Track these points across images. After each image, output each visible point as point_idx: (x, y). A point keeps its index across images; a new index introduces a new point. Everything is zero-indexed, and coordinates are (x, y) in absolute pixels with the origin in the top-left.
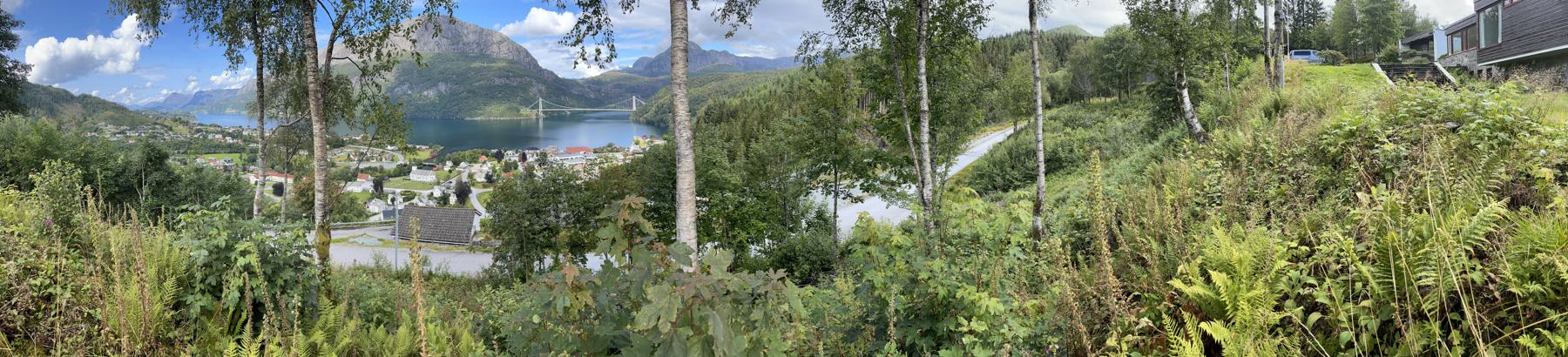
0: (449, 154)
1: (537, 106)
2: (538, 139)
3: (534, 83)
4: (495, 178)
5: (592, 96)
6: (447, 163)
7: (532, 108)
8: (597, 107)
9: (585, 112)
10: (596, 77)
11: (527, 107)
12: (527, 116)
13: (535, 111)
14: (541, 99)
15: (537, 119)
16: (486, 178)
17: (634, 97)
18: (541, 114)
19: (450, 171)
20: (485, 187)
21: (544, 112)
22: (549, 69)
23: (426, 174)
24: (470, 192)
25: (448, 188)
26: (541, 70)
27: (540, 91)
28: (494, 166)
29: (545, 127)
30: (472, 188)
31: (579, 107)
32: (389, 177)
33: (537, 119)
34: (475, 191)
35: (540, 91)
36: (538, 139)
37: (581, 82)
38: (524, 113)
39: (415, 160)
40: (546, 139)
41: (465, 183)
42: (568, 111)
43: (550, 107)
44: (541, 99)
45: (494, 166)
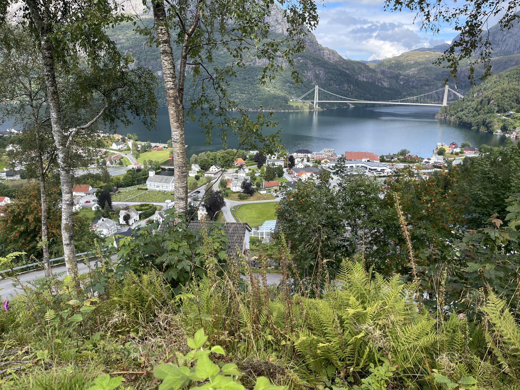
0: (194, 156)
1: (311, 97)
2: (308, 139)
3: (310, 64)
4: (255, 187)
5: (386, 84)
6: (193, 166)
7: (305, 98)
8: (388, 100)
9: (374, 105)
10: (395, 58)
11: (298, 96)
12: (297, 107)
13: (308, 103)
14: (317, 87)
15: (311, 113)
16: (242, 187)
17: (447, 86)
18: (316, 107)
19: (197, 178)
20: (241, 198)
21: (320, 104)
22: (330, 48)
23: (167, 182)
24: (223, 204)
25: (195, 200)
26: (320, 49)
27: (317, 76)
28: (254, 172)
29: (322, 124)
30: (225, 200)
31: (365, 100)
32: (120, 186)
33: (311, 113)
34: (229, 203)
35: (317, 76)
36: (308, 139)
37: (372, 66)
38: (294, 105)
39: (151, 162)
40: (320, 139)
41: (218, 193)
42: (351, 102)
43: (326, 98)
44: (317, 87)
45: (254, 172)
